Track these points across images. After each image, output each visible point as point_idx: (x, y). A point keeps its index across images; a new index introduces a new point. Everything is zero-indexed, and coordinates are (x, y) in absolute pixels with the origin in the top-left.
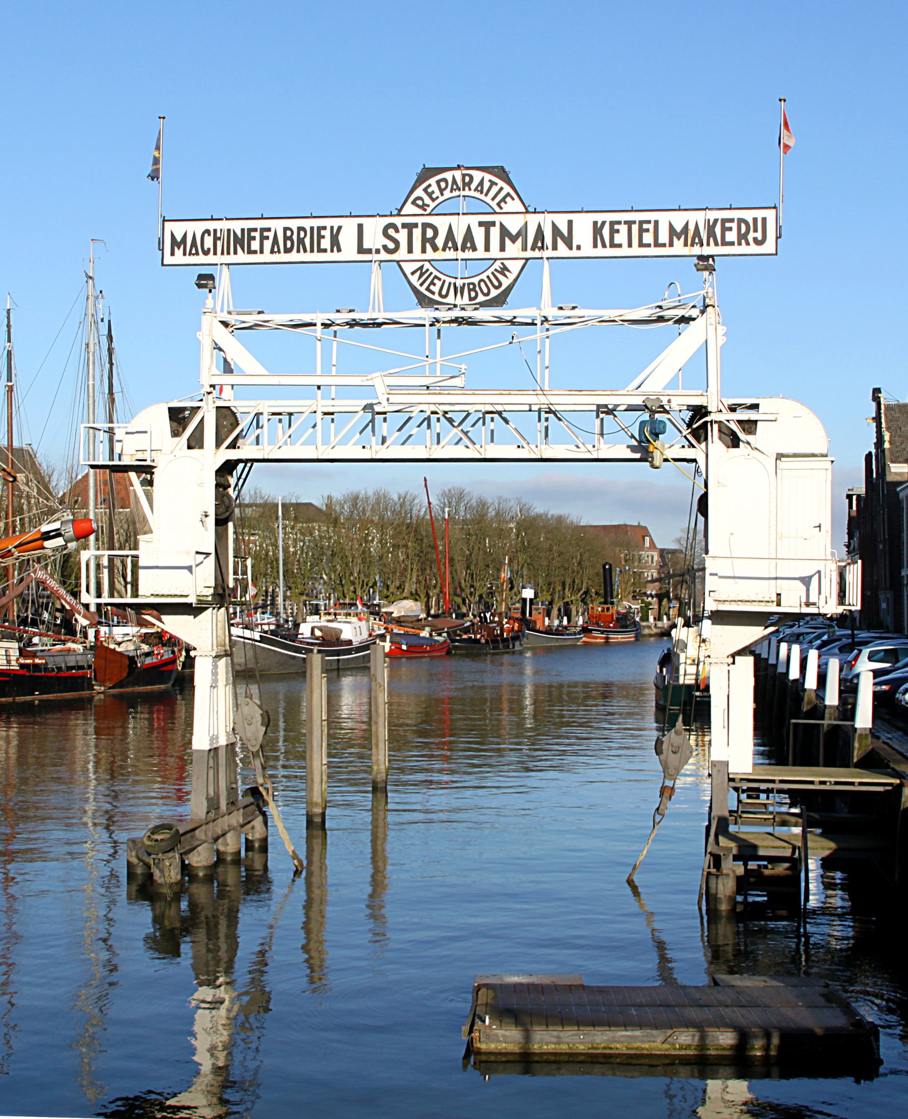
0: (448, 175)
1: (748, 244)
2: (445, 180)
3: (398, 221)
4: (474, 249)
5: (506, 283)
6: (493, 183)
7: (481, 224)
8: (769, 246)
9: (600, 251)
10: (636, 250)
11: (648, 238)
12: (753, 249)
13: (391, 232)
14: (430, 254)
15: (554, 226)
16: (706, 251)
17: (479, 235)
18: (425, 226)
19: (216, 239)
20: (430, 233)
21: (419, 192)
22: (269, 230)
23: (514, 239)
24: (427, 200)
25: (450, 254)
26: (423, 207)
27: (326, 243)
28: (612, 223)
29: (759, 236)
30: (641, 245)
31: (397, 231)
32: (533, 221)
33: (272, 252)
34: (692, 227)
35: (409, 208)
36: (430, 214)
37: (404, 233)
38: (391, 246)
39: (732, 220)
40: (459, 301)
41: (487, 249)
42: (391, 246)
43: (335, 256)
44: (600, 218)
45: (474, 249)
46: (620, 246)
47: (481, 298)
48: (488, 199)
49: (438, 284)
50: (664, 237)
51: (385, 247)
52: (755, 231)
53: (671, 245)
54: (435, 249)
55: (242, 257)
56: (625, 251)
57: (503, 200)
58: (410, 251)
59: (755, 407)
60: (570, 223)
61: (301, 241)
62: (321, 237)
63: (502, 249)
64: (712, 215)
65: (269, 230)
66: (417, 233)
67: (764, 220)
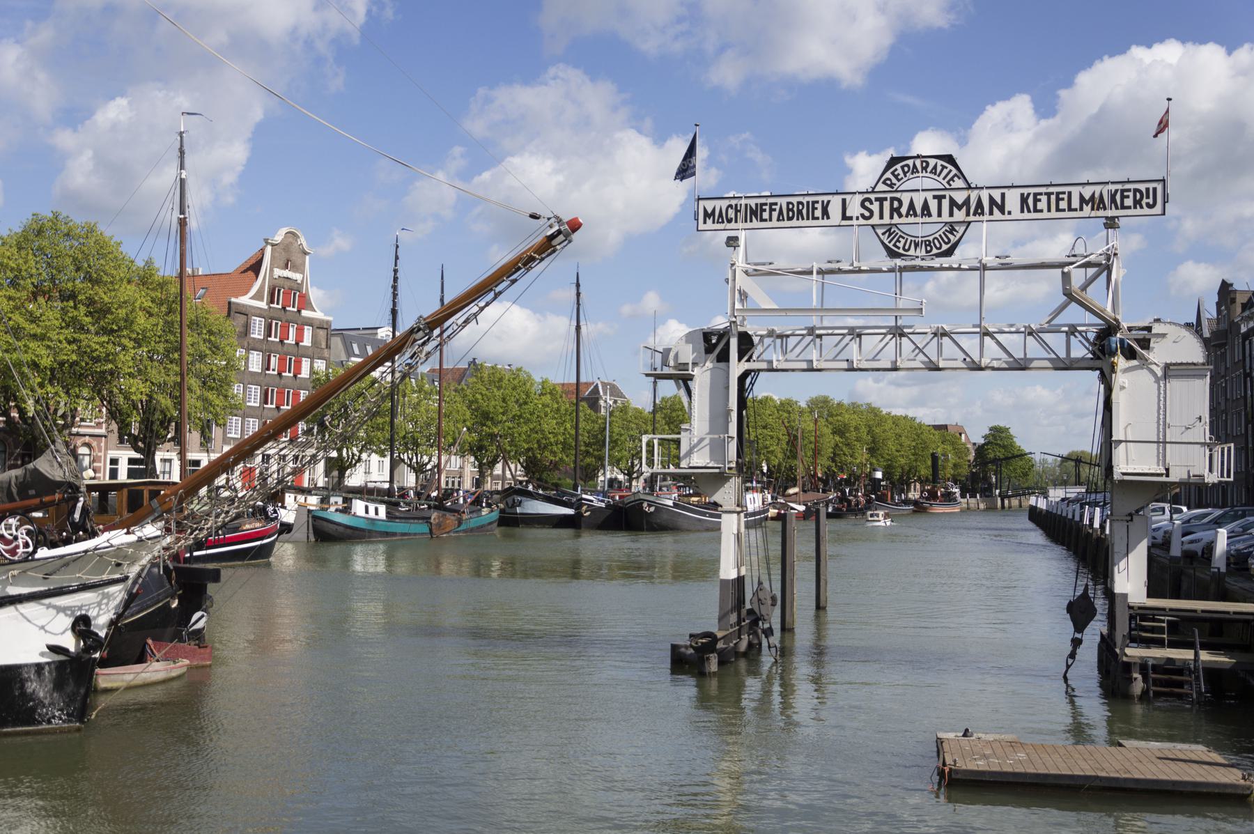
0: (910, 162)
1: (1141, 207)
2: (908, 166)
3: (872, 197)
4: (930, 215)
5: (953, 239)
6: (944, 167)
7: (935, 197)
8: (1158, 209)
9: (1026, 215)
10: (1054, 214)
11: (1063, 205)
12: (1146, 211)
13: (867, 204)
14: (896, 220)
15: (991, 198)
16: (1109, 213)
17: (933, 205)
18: (893, 199)
19: (737, 211)
20: (896, 204)
21: (888, 175)
22: (776, 204)
23: (960, 208)
24: (894, 181)
25: (911, 219)
26: (891, 185)
27: (818, 213)
28: (1035, 195)
29: (1151, 201)
30: (1058, 210)
31: (871, 203)
32: (974, 195)
33: (778, 220)
34: (1097, 195)
35: (881, 187)
36: (896, 191)
37: (877, 204)
38: (867, 214)
39: (1129, 190)
40: (918, 253)
41: (940, 215)
42: (867, 214)
43: (825, 222)
44: (1026, 191)
45: (930, 215)
46: (1041, 211)
47: (935, 251)
48: (940, 179)
49: (903, 241)
50: (1076, 204)
51: (862, 215)
52: (1148, 197)
53: (1081, 209)
54: (900, 216)
55: (756, 224)
56: (1045, 214)
57: (952, 179)
58: (881, 217)
59: (1149, 329)
60: (1003, 195)
61: (800, 212)
62: (814, 209)
63: (951, 214)
64: (1113, 187)
65: (776, 204)
66: (887, 204)
67: (1155, 190)
